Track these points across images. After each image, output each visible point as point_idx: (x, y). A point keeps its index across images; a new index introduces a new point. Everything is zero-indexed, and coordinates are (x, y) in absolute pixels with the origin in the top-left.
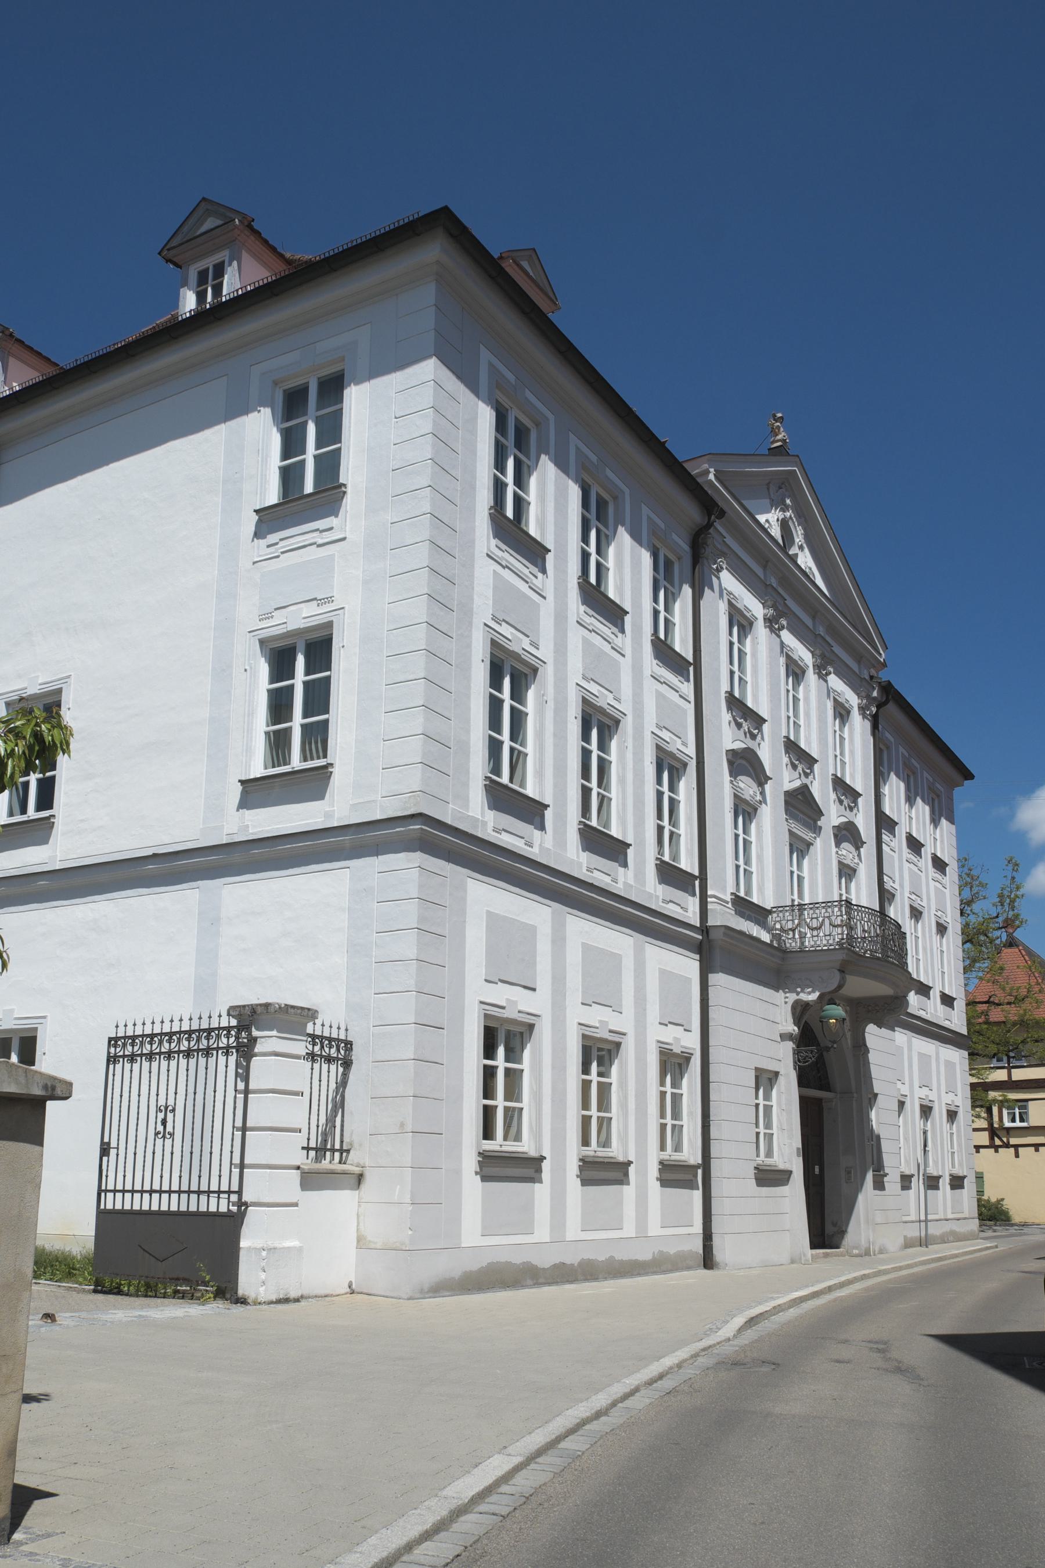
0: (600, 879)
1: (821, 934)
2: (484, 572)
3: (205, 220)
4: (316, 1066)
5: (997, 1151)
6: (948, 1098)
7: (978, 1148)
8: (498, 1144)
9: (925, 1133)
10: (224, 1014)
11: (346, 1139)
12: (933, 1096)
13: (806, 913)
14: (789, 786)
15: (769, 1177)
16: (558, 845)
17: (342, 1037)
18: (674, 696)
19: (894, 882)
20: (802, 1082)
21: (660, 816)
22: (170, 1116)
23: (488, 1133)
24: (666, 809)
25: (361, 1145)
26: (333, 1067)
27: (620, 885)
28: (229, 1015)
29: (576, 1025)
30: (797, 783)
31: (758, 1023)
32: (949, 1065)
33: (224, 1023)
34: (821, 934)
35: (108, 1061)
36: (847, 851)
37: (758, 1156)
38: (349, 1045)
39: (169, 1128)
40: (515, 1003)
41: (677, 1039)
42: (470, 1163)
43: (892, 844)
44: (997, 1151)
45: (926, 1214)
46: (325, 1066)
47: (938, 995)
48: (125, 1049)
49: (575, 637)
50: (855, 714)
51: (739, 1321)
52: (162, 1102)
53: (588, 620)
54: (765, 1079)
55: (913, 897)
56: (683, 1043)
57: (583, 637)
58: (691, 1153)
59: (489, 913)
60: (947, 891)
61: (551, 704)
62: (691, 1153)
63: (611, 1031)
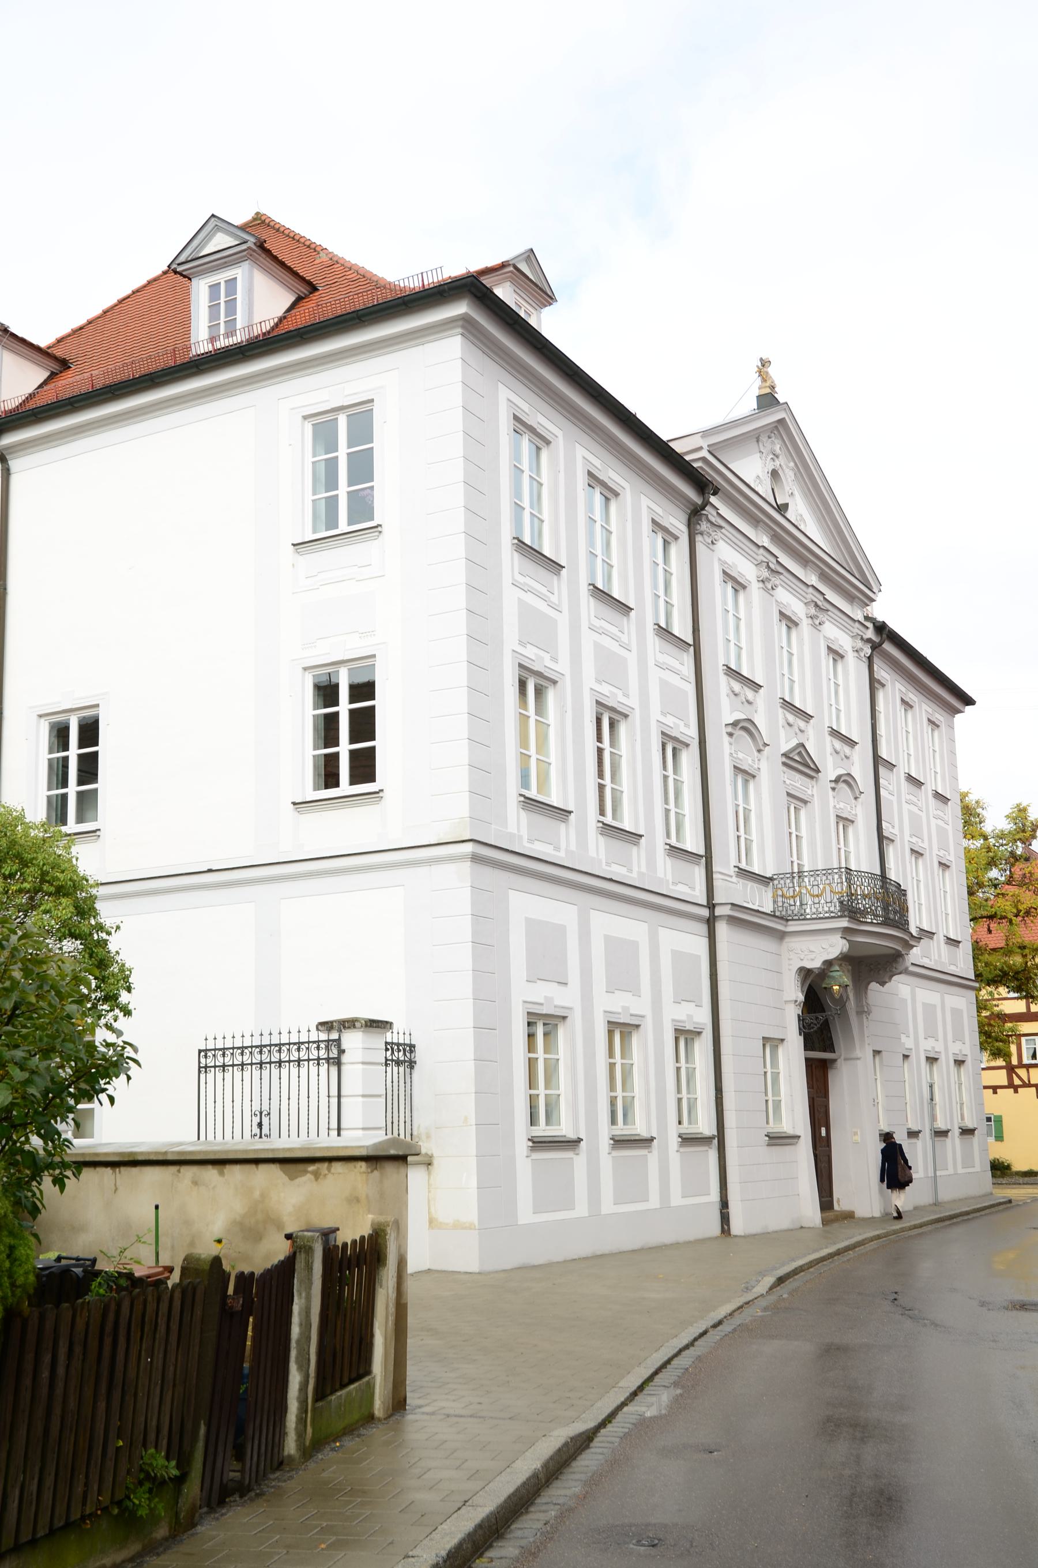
0: (617, 871)
1: (822, 901)
2: (511, 598)
3: (214, 235)
4: (389, 1069)
5: (1016, 1091)
6: (956, 1049)
7: (995, 1089)
8: (542, 1130)
9: (931, 1086)
10: (313, 1029)
11: (415, 1133)
12: (939, 1047)
13: (806, 880)
14: (785, 748)
15: (777, 1140)
16: (580, 844)
17: (407, 1042)
18: (674, 680)
19: (893, 827)
20: (808, 1046)
21: (666, 802)
22: (265, 1121)
23: (533, 1120)
24: (671, 792)
25: (428, 1137)
26: (401, 1069)
27: (634, 875)
28: (318, 1029)
29: (602, 1013)
30: (794, 743)
31: (766, 993)
32: (956, 1012)
33: (314, 1037)
34: (822, 901)
35: (200, 1072)
36: (841, 802)
37: (767, 1123)
38: (412, 1047)
39: (265, 1130)
40: (552, 998)
41: (690, 1017)
42: (522, 1145)
43: (891, 788)
44: (1016, 1091)
45: (935, 1171)
46: (395, 1069)
47: (942, 939)
48: (210, 1060)
49: (588, 640)
50: (851, 657)
51: (770, 1280)
52: (256, 1107)
53: (598, 623)
54: (772, 1043)
55: (914, 840)
56: (695, 1020)
57: (595, 642)
58: (705, 1126)
59: (526, 918)
60: (949, 828)
61: (569, 715)
62: (705, 1126)
63: (632, 1015)
